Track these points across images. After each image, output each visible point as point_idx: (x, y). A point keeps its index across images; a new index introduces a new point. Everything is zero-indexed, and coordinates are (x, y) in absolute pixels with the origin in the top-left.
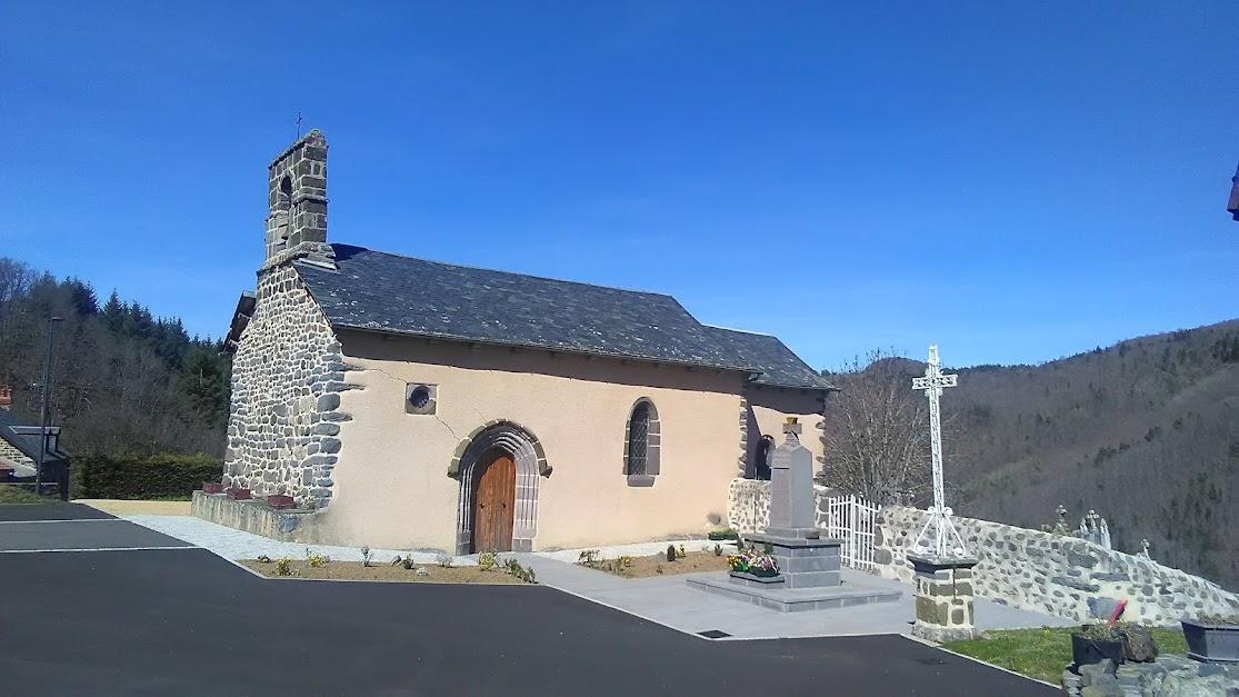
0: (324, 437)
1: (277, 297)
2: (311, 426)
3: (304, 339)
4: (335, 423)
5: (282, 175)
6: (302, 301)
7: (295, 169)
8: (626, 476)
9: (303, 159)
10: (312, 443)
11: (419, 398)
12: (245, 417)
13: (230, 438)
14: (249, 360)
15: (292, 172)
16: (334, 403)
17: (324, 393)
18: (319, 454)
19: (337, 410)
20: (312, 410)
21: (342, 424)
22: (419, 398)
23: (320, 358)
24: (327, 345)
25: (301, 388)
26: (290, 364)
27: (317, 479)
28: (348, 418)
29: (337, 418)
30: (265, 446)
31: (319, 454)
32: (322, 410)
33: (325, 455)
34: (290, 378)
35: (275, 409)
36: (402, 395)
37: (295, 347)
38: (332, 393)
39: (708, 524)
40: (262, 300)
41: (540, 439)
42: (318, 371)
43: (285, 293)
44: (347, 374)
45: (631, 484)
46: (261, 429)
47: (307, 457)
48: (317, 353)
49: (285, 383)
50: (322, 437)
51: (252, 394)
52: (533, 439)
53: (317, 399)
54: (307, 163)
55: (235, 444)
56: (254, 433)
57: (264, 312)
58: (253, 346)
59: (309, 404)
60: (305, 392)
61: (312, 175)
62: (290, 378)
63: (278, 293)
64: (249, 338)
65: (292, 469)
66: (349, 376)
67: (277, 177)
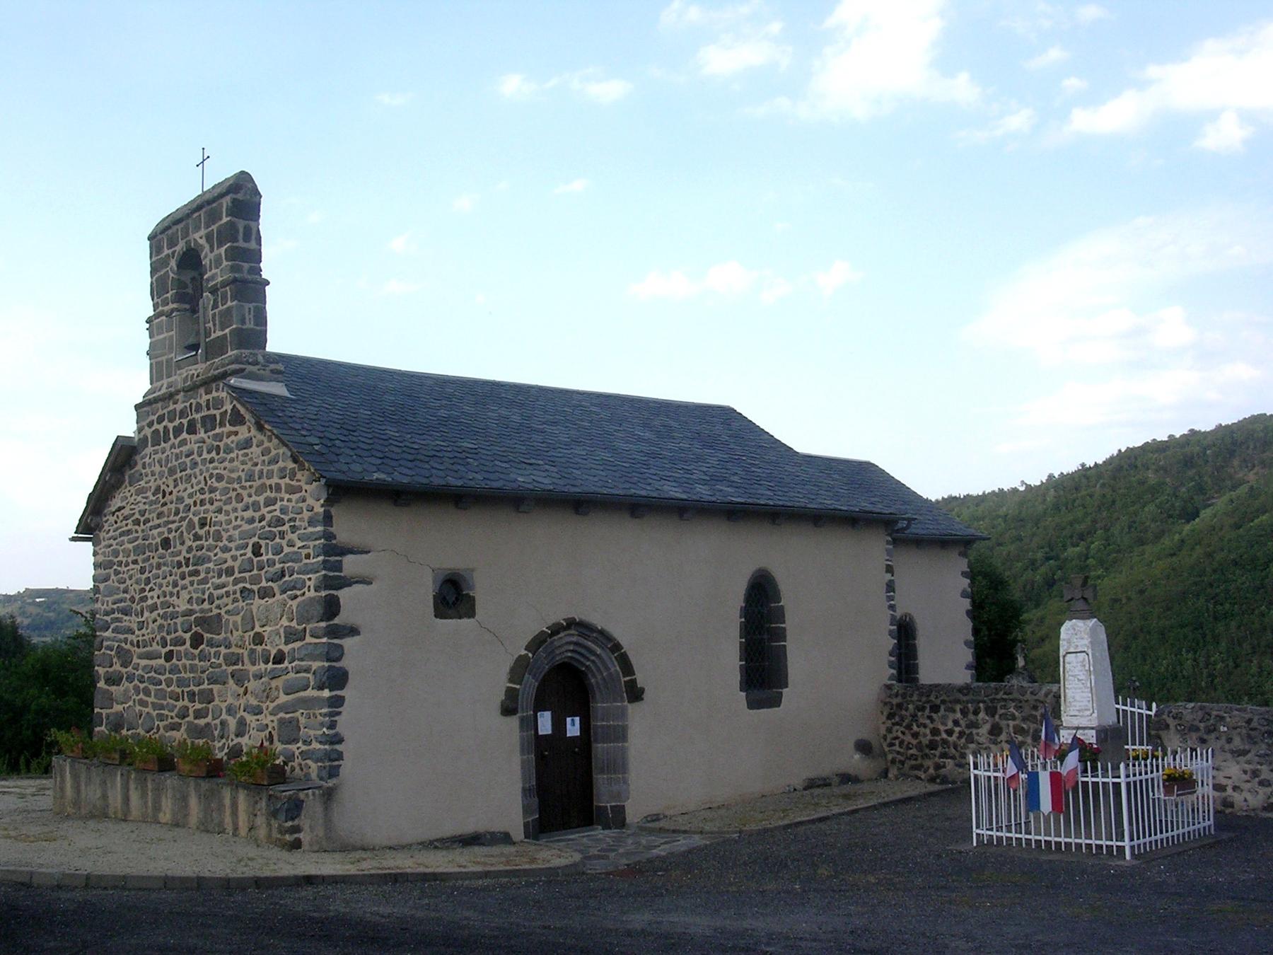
0: (320, 664)
1: (184, 442)
2: (286, 649)
3: (256, 506)
4: (336, 641)
5: (180, 247)
6: (247, 444)
7: (209, 238)
8: (744, 694)
9: (225, 220)
10: (292, 675)
11: (453, 597)
12: (130, 637)
13: (101, 670)
14: (130, 546)
15: (202, 242)
16: (331, 608)
17: (312, 594)
18: (310, 693)
19: (336, 621)
20: (285, 622)
21: (347, 643)
22: (453, 597)
23: (294, 537)
24: (306, 515)
25: (255, 588)
26: (226, 550)
27: (312, 733)
28: (353, 631)
29: (334, 632)
30: (181, 683)
31: (310, 693)
32: (308, 621)
33: (326, 693)
34: (230, 572)
35: (199, 622)
36: (427, 590)
37: (235, 523)
38: (323, 593)
39: (857, 756)
40: (149, 449)
41: (626, 646)
42: (295, 558)
43: (202, 434)
44: (348, 560)
45: (752, 704)
46: (169, 656)
47: (283, 698)
48: (286, 528)
49: (216, 581)
50: (316, 665)
51: (144, 599)
52: (617, 647)
53: (295, 603)
54: (231, 225)
55: (114, 680)
56: (153, 663)
57: (157, 469)
58: (137, 522)
59: (276, 617)
60: (265, 593)
61: (241, 244)
62: (230, 572)
63: (184, 435)
64: (126, 512)
65: (249, 718)
66: (351, 564)
67: (166, 252)
